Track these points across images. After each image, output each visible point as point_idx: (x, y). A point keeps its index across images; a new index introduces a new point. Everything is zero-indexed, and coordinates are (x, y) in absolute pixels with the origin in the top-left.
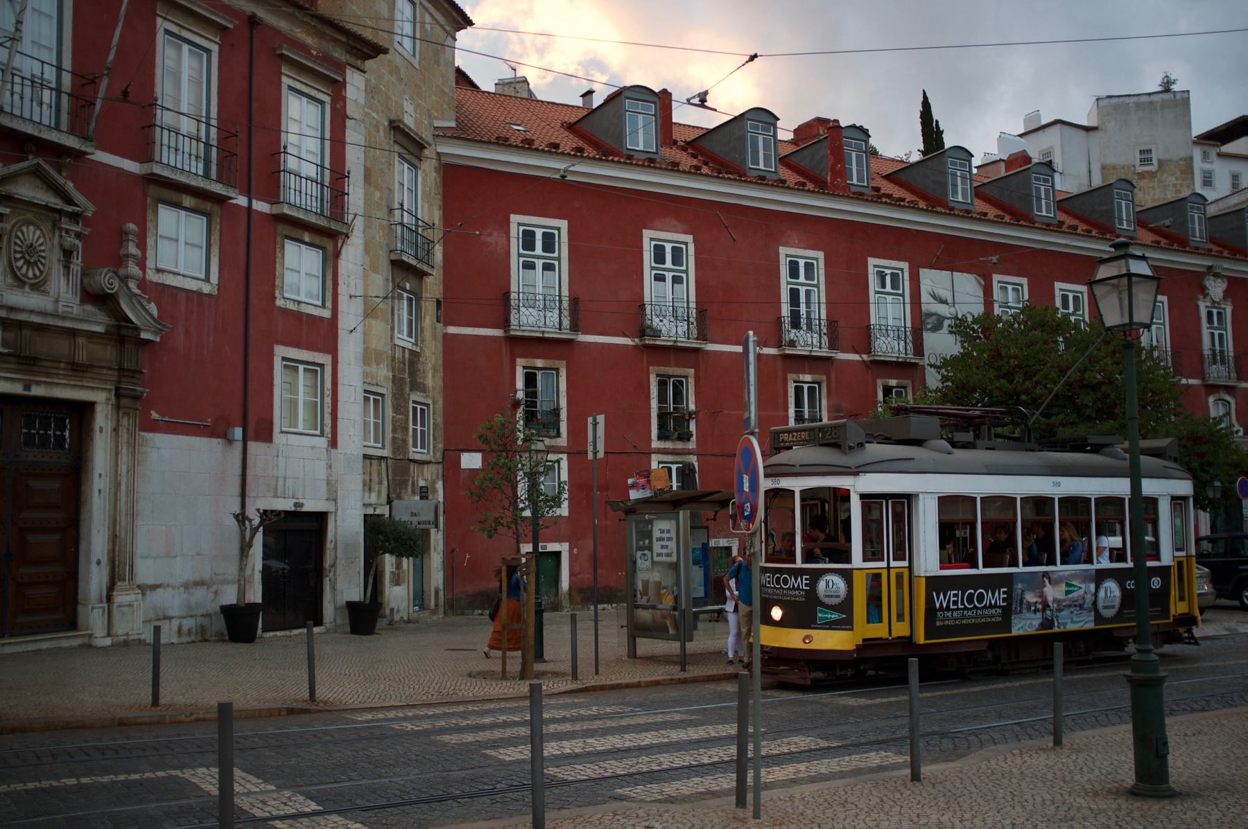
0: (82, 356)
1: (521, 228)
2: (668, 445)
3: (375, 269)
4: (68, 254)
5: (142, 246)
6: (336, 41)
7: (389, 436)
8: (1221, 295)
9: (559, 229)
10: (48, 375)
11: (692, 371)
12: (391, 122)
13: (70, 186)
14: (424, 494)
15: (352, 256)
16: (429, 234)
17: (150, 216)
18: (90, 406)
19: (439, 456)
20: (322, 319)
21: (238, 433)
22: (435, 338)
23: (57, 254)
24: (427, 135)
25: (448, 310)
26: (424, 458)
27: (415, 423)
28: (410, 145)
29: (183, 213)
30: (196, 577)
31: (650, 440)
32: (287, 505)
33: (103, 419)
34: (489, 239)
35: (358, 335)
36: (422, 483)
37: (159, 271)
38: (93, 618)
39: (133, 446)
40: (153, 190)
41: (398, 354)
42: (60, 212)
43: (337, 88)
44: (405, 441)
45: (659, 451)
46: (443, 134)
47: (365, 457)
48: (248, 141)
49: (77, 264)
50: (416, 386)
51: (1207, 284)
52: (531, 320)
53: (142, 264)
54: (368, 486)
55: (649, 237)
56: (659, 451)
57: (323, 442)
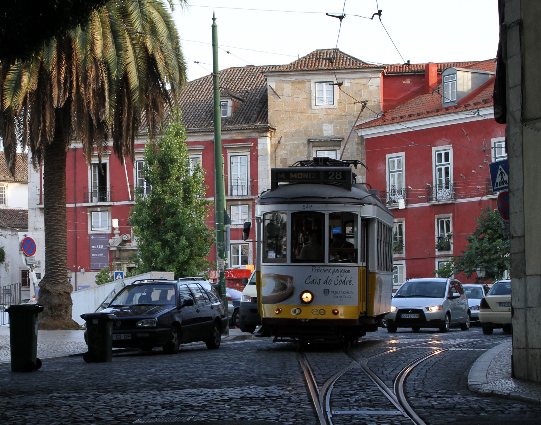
2: (443, 253)
11: (452, 214)
45: (439, 257)
56: (439, 257)
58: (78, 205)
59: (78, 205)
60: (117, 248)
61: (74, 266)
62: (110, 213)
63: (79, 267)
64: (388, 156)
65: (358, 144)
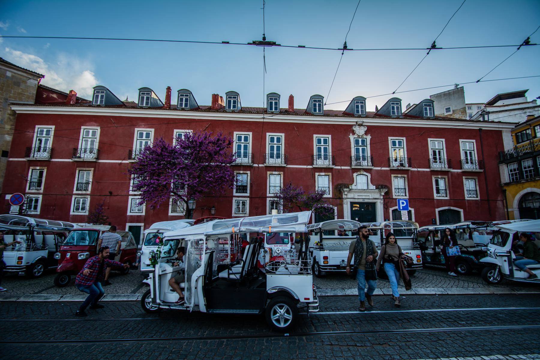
2: (80, 192)
8: (364, 133)
11: (93, 169)
31: (73, 191)
45: (76, 194)
51: (354, 128)
65: (10, 115)
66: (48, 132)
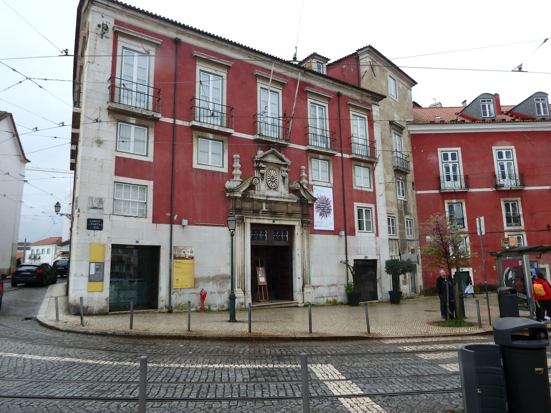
0: (290, 211)
1: (442, 153)
3: (388, 173)
4: (284, 178)
5: (307, 173)
6: (367, 96)
7: (398, 231)
9: (457, 151)
10: (280, 217)
12: (390, 122)
13: (283, 156)
14: (413, 251)
15: (379, 169)
16: (408, 159)
17: (309, 163)
18: (294, 226)
19: (418, 238)
20: (370, 192)
21: (343, 233)
22: (413, 195)
23: (281, 178)
24: (404, 124)
25: (417, 185)
26: (412, 239)
27: (407, 226)
28: (397, 128)
29: (320, 161)
30: (332, 283)
32: (362, 257)
33: (298, 231)
34: (430, 158)
35: (383, 197)
36: (412, 248)
37: (313, 181)
38: (298, 297)
39: (308, 239)
40: (310, 154)
41: (399, 202)
42: (281, 164)
43: (369, 112)
44: (404, 233)
46: (409, 123)
47: (389, 239)
48: (340, 135)
49: (287, 180)
50: (407, 213)
52: (449, 186)
53: (307, 179)
54: (391, 250)
55: (495, 150)
57: (373, 235)
58: (179, 122)
59: (179, 122)
60: (242, 195)
61: (169, 214)
62: (226, 145)
63: (175, 217)
64: (439, 149)
66: (454, 156)
